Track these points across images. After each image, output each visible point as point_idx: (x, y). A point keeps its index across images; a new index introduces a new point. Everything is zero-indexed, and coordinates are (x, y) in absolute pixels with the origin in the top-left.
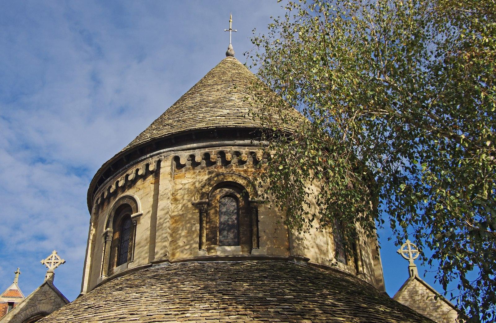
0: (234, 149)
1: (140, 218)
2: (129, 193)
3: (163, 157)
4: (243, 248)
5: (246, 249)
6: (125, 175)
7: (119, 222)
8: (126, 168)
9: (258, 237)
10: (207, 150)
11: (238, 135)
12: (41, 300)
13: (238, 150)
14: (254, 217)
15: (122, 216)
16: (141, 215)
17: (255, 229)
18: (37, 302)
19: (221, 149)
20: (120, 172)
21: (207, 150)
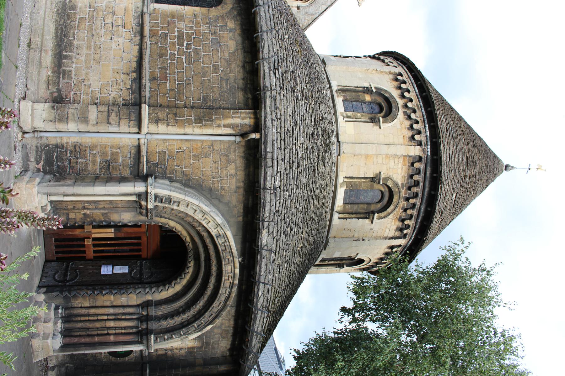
0: (418, 204)
1: (377, 126)
2: (401, 115)
3: (423, 147)
4: (341, 206)
5: (339, 209)
6: (416, 109)
8: (422, 110)
9: (346, 218)
10: (421, 184)
11: (429, 209)
13: (416, 207)
14: (362, 216)
15: (383, 104)
16: (380, 128)
17: (353, 216)
19: (420, 195)
20: (420, 103)
21: (421, 184)
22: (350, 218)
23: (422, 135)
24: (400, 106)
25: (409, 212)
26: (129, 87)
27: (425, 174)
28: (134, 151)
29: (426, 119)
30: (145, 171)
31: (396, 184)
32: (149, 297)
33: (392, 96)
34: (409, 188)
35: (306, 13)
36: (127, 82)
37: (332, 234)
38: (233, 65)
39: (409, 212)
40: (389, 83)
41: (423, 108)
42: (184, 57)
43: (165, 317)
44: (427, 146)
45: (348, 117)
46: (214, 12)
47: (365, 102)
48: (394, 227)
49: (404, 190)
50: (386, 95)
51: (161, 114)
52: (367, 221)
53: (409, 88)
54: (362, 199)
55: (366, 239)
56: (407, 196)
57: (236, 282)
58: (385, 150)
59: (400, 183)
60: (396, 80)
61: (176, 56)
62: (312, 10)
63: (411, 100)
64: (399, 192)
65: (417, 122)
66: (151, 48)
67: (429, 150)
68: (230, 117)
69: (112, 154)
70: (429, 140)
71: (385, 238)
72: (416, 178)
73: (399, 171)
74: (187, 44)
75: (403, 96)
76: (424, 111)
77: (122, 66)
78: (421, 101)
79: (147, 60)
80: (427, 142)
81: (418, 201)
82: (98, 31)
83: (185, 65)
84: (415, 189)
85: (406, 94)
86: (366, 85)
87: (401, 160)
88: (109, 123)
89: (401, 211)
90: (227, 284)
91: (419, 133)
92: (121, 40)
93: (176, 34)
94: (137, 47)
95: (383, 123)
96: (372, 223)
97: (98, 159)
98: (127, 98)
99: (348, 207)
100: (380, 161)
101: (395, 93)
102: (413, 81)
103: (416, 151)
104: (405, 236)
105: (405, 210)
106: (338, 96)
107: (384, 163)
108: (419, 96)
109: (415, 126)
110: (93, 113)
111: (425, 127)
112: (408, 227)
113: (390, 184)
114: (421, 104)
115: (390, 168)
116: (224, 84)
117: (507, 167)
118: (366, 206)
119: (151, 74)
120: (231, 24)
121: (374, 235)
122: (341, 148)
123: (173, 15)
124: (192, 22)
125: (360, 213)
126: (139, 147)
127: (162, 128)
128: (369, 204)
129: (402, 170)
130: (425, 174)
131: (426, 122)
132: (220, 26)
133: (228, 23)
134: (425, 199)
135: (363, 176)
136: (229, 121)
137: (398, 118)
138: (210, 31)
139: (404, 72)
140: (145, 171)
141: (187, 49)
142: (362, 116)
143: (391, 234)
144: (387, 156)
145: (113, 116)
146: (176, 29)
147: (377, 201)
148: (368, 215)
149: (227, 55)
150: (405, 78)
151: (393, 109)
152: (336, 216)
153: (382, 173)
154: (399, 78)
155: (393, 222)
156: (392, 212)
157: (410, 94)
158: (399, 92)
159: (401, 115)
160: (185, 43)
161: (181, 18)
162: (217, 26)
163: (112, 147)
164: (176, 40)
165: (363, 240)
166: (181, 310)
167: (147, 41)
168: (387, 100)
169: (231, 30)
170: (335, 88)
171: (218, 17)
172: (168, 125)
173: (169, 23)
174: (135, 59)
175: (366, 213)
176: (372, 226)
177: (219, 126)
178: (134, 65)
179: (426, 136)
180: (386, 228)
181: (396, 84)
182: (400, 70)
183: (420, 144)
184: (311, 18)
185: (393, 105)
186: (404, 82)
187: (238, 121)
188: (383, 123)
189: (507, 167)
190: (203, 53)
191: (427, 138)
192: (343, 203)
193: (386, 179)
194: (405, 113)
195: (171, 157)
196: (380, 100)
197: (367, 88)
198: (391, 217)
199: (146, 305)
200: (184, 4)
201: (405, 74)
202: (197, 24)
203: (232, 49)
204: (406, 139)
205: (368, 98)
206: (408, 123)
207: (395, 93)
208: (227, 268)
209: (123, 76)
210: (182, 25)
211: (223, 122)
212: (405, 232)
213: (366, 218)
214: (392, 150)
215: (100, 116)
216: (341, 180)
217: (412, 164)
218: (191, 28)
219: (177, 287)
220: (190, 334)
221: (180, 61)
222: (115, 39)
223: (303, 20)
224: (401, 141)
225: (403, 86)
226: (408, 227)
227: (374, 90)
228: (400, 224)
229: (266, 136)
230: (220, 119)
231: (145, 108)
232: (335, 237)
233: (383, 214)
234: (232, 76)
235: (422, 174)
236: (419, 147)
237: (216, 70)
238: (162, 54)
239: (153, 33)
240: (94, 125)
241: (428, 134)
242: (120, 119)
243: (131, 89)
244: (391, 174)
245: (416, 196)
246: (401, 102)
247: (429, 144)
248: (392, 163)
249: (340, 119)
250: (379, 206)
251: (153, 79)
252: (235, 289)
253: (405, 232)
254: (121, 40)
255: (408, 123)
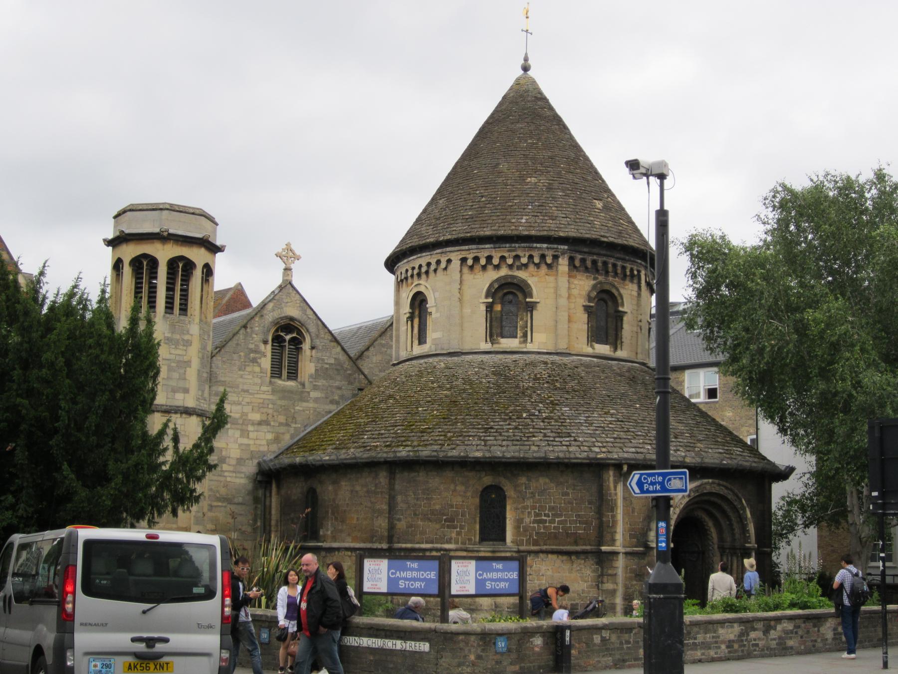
1: (536, 307)
2: (522, 274)
6: (514, 254)
7: (500, 294)
9: (622, 342)
10: (595, 257)
12: (287, 303)
14: (619, 324)
15: (505, 291)
18: (283, 305)
19: (605, 259)
21: (595, 257)
22: (621, 338)
23: (546, 253)
24: (510, 273)
25: (619, 271)
26: (583, 561)
27: (585, 253)
28: (629, 557)
29: (528, 245)
30: (641, 549)
31: (594, 287)
32: (716, 546)
33: (497, 280)
34: (597, 271)
35: (317, 336)
36: (579, 564)
37: (633, 358)
38: (561, 480)
39: (619, 271)
40: (476, 277)
41: (513, 245)
42: (557, 519)
43: (733, 534)
44: (557, 248)
45: (525, 335)
46: (510, 492)
47: (501, 311)
48: (630, 285)
49: (600, 277)
50: (496, 286)
51: (608, 537)
52: (625, 318)
53: (486, 255)
54: (603, 323)
55: (640, 317)
56: (603, 272)
57: (717, 481)
58: (563, 302)
59: (593, 282)
60: (471, 268)
61: (556, 525)
62: (313, 329)
63: (503, 258)
64: (600, 283)
65: (531, 257)
66: (550, 545)
67: (562, 247)
68: (609, 486)
69: (630, 573)
70: (552, 246)
71: (639, 295)
72: (589, 264)
73: (581, 283)
74: (545, 516)
75: (497, 267)
76: (517, 245)
77: (567, 566)
78: (504, 245)
79: (562, 547)
80: (554, 248)
81: (612, 261)
82: (537, 585)
83: (563, 518)
84: (600, 264)
85: (496, 261)
86: (483, 308)
87: (572, 280)
88: (616, 575)
89: (617, 279)
90: (717, 488)
91: (543, 257)
92: (543, 568)
93: (536, 525)
94: (550, 556)
95: (532, 297)
96: (626, 313)
97: (635, 582)
98: (592, 562)
99: (611, 339)
100: (572, 306)
101: (492, 275)
102: (474, 246)
103: (563, 262)
104: (639, 272)
105: (616, 274)
106: (498, 343)
107: (574, 301)
108: (497, 245)
109: (537, 260)
110: (609, 586)
111: (536, 248)
112: (632, 270)
113: (594, 294)
114: (508, 245)
115: (579, 294)
116: (578, 488)
117: (526, 69)
118: (610, 320)
119: (571, 544)
120: (523, 480)
121: (635, 307)
122: (564, 351)
123: (517, 527)
124: (523, 512)
125: (616, 326)
126: (626, 554)
127: (619, 537)
128: (607, 315)
129: (580, 280)
130: (585, 253)
131: (531, 245)
132: (525, 488)
133: (522, 482)
134: (609, 253)
135: (586, 326)
136: (612, 485)
137: (526, 279)
138: (531, 497)
139: (459, 253)
140: (641, 549)
141: (549, 516)
142: (522, 319)
143: (635, 287)
144: (569, 297)
145: (610, 572)
146: (532, 525)
147: (605, 305)
148: (619, 317)
149: (552, 485)
150: (470, 256)
151: (515, 281)
152: (620, 354)
153: (584, 304)
154: (470, 262)
155: (627, 287)
156: (618, 290)
157: (495, 257)
158: (490, 267)
159: (522, 274)
160: (543, 518)
161: (519, 522)
162: (526, 492)
163: (626, 573)
164: (541, 525)
165: (640, 321)
166: (728, 523)
167: (544, 548)
168: (501, 287)
169: (529, 480)
170: (488, 347)
171: (515, 490)
172: (615, 532)
173: (525, 530)
174: (560, 557)
175: (617, 320)
176: (629, 311)
177: (616, 494)
178: (565, 558)
179: (548, 248)
180: (630, 294)
181: (477, 268)
182: (456, 258)
183: (556, 257)
184: (322, 332)
185: (509, 280)
186: (476, 259)
187: (611, 479)
188: (532, 297)
189: (526, 69)
190: (552, 504)
191: (551, 248)
192: (606, 344)
193: (590, 299)
194: (519, 268)
195: (633, 530)
196: (500, 294)
197: (487, 307)
198: (622, 291)
199: (722, 550)
200: (505, 518)
201: (463, 253)
202: (525, 508)
203: (547, 480)
204: (550, 272)
205: (498, 308)
206: (532, 268)
207: (492, 275)
208: (708, 489)
209: (575, 566)
210: (527, 520)
211: (613, 491)
212: (636, 273)
213: (622, 320)
214: (564, 292)
215: (610, 581)
216: (589, 350)
217: (575, 267)
218: (529, 513)
219: (710, 524)
220: (746, 515)
221: (559, 522)
222: (543, 572)
223: (325, 341)
224: (551, 279)
225: (483, 262)
226: (632, 270)
227: (490, 300)
228: (628, 278)
229: (626, 459)
230: (611, 493)
231: (604, 548)
232: (637, 353)
233: (620, 301)
234: (570, 482)
235: (586, 256)
236: (560, 260)
237: (567, 494)
238: (554, 537)
239: (536, 543)
240: (617, 585)
241: (545, 246)
242: (612, 567)
243: (584, 559)
244: (584, 293)
245: (605, 263)
246: (504, 272)
247: (555, 246)
248: (575, 292)
249: (530, 347)
250: (610, 303)
251: (576, 543)
252: (721, 482)
253: (636, 273)
254: (543, 568)
255: (532, 268)
